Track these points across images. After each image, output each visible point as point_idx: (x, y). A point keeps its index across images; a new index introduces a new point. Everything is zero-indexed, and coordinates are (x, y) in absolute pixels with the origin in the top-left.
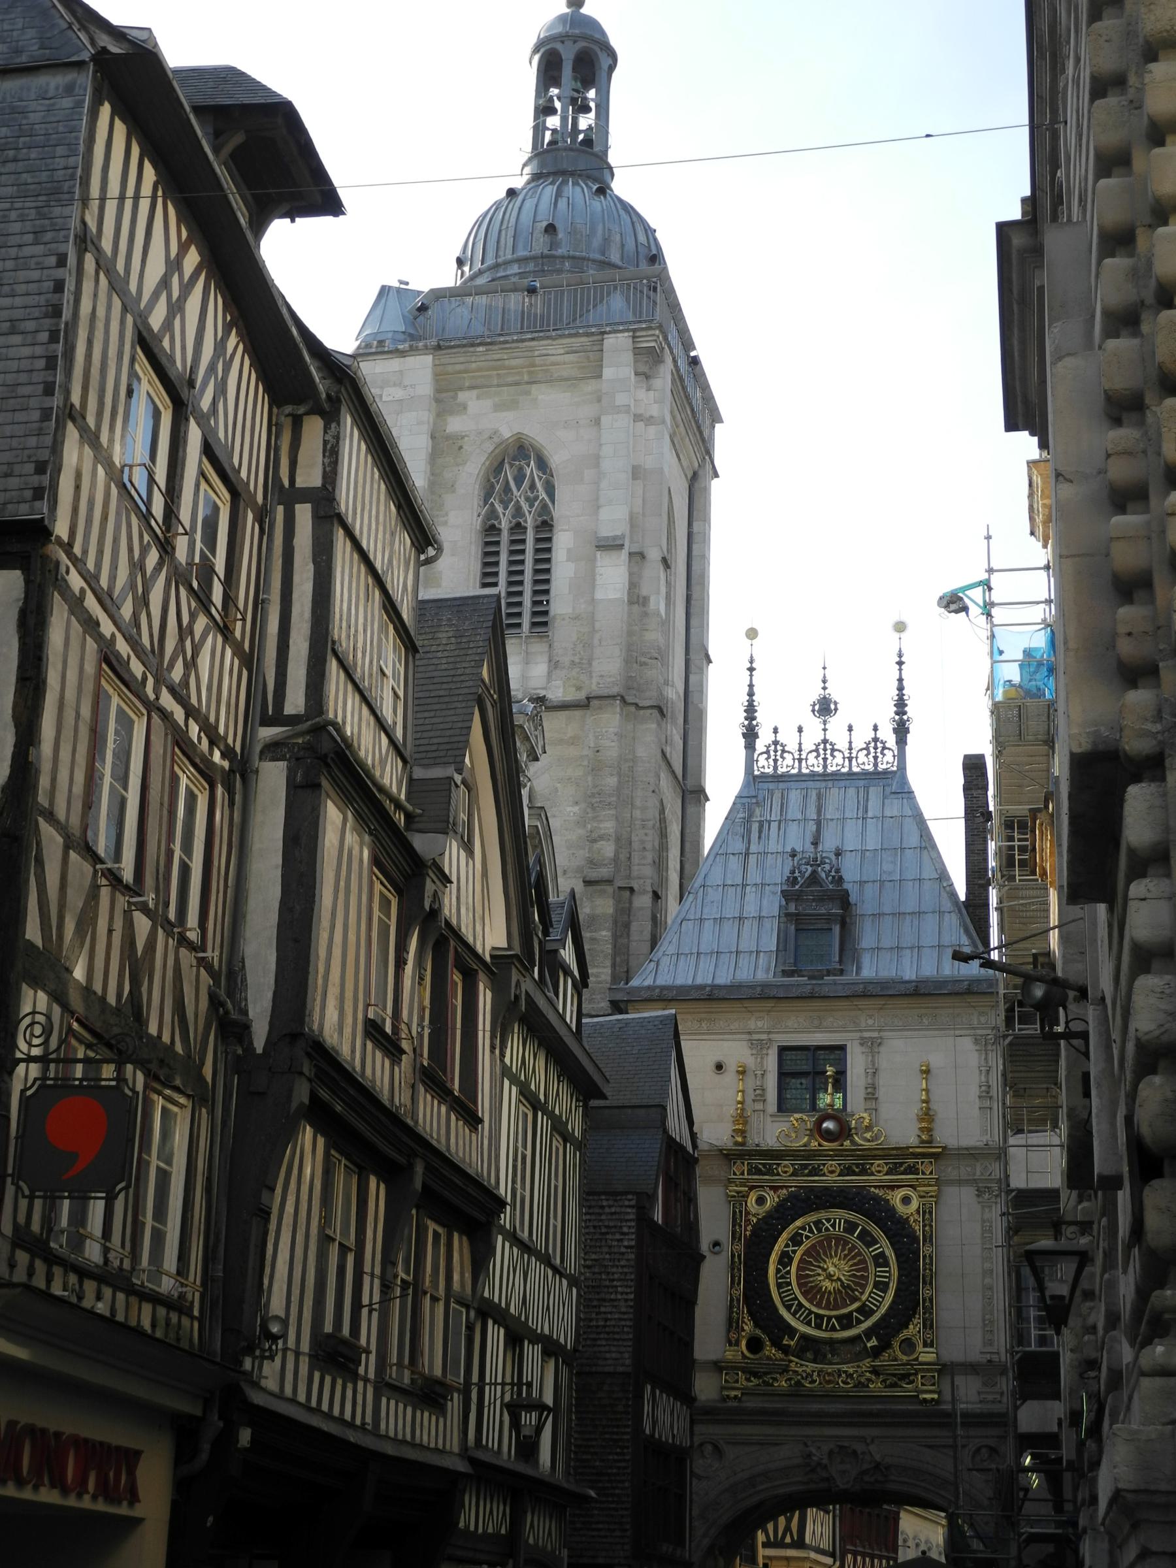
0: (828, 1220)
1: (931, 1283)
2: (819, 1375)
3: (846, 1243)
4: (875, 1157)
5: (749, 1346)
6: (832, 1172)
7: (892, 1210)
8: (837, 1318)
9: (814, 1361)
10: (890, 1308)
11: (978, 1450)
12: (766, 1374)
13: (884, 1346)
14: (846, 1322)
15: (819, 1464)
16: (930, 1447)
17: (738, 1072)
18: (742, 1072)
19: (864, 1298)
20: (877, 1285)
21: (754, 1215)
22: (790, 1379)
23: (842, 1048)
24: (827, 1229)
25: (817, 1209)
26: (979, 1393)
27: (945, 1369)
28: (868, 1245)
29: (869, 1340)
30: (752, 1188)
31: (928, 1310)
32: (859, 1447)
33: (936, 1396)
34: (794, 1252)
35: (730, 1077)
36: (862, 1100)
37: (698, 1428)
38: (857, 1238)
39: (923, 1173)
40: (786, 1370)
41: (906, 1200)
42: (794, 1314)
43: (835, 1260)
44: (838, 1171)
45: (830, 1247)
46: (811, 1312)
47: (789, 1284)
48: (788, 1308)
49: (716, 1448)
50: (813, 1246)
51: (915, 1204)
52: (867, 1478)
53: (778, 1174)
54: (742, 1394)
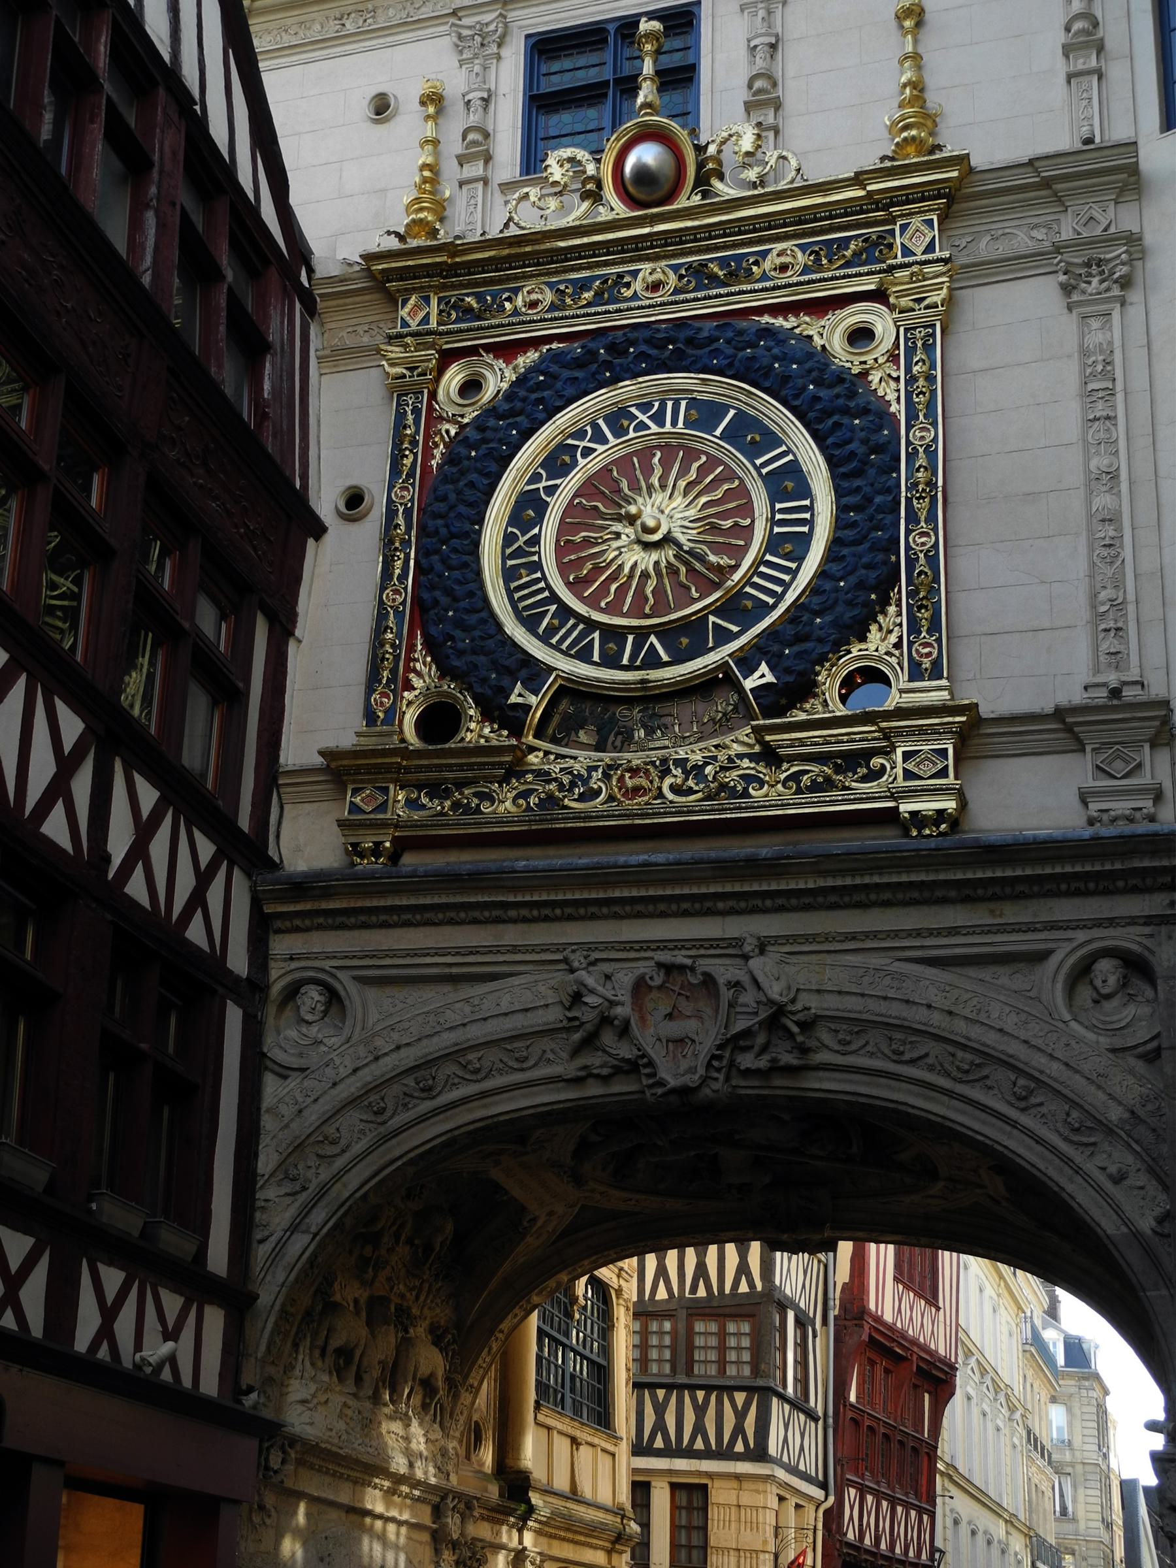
0: (645, 407)
1: (932, 518)
2: (607, 777)
3: (691, 454)
5: (421, 724)
7: (817, 362)
8: (662, 632)
9: (600, 747)
10: (813, 589)
12: (460, 785)
13: (795, 689)
14: (688, 637)
19: (737, 576)
20: (773, 544)
21: (452, 420)
22: (525, 795)
24: (642, 426)
25: (614, 381)
26: (1084, 798)
28: (753, 450)
29: (749, 671)
30: (447, 358)
31: (925, 598)
32: (724, 971)
33: (950, 805)
34: (551, 490)
36: (741, 108)
42: (545, 639)
43: (659, 497)
45: (648, 471)
46: (591, 625)
47: (538, 566)
48: (530, 623)
50: (606, 470)
52: (747, 1061)
53: (516, 312)
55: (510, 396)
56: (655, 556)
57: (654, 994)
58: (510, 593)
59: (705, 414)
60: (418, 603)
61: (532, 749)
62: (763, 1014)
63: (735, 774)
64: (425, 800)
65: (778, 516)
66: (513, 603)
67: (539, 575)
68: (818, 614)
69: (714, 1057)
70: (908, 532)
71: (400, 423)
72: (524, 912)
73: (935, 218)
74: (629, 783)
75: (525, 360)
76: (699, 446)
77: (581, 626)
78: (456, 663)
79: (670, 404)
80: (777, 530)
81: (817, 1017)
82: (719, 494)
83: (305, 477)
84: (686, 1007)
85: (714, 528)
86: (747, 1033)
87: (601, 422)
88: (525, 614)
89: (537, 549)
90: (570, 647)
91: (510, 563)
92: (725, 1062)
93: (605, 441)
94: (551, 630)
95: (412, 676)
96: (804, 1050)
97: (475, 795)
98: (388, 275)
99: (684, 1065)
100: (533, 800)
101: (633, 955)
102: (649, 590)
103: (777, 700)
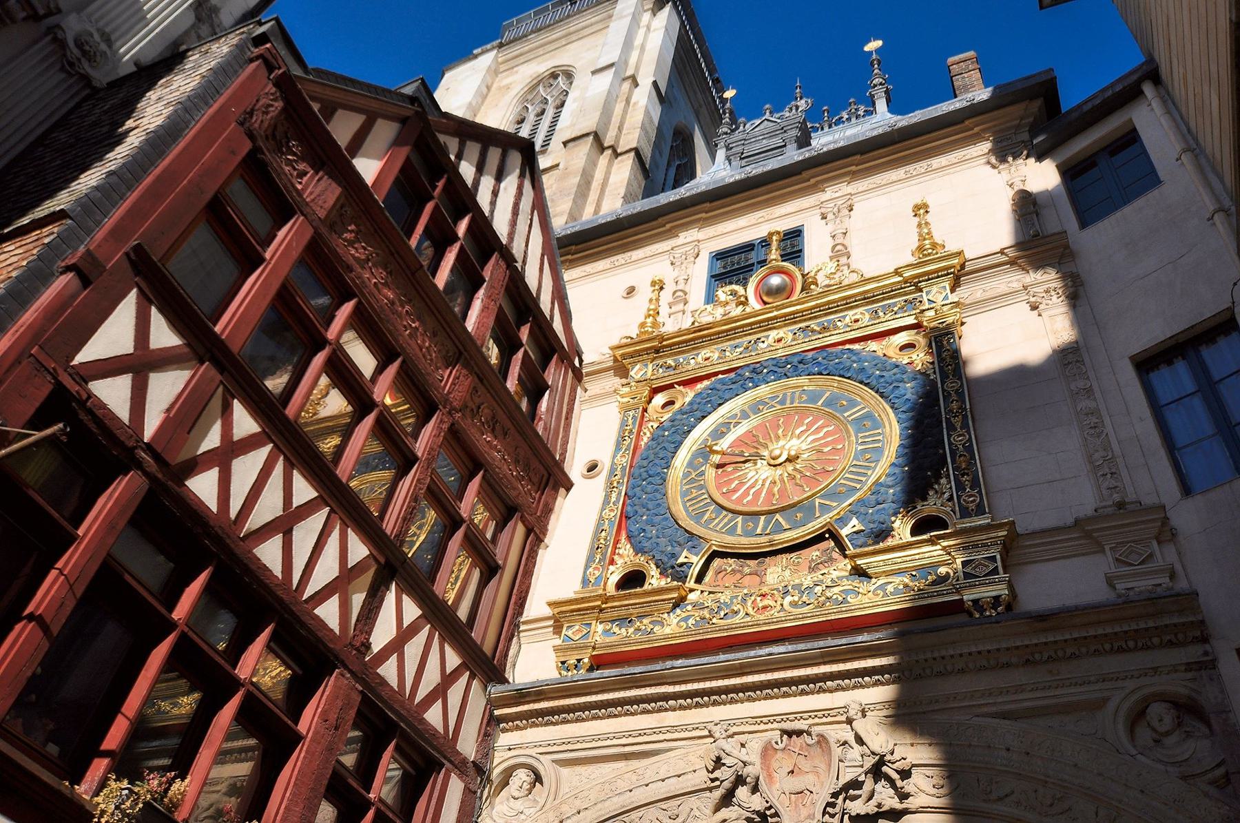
1: (965, 426)
4: (848, 304)
7: (883, 363)
11: (1138, 716)
12: (641, 617)
15: (740, 780)
16: (1004, 716)
17: (653, 283)
18: (659, 286)
22: (686, 619)
23: (795, 235)
30: (656, 391)
33: (1002, 590)
35: (645, 293)
37: (505, 739)
40: (679, 603)
44: (790, 336)
48: (698, 517)
49: (538, 778)
54: (592, 657)
55: (691, 403)
56: (779, 471)
57: (779, 754)
59: (814, 397)
60: (625, 516)
61: (692, 590)
62: (870, 762)
63: (836, 590)
64: (616, 629)
68: (890, 487)
69: (829, 804)
70: (949, 436)
71: (624, 424)
72: (681, 701)
75: (700, 386)
78: (647, 544)
80: (860, 448)
81: (914, 766)
82: (821, 434)
83: (563, 454)
84: (804, 764)
85: (819, 451)
86: (856, 784)
92: (837, 809)
95: (616, 557)
96: (903, 796)
98: (624, 356)
99: (804, 812)
100: (691, 621)
101: (762, 727)
102: (776, 489)
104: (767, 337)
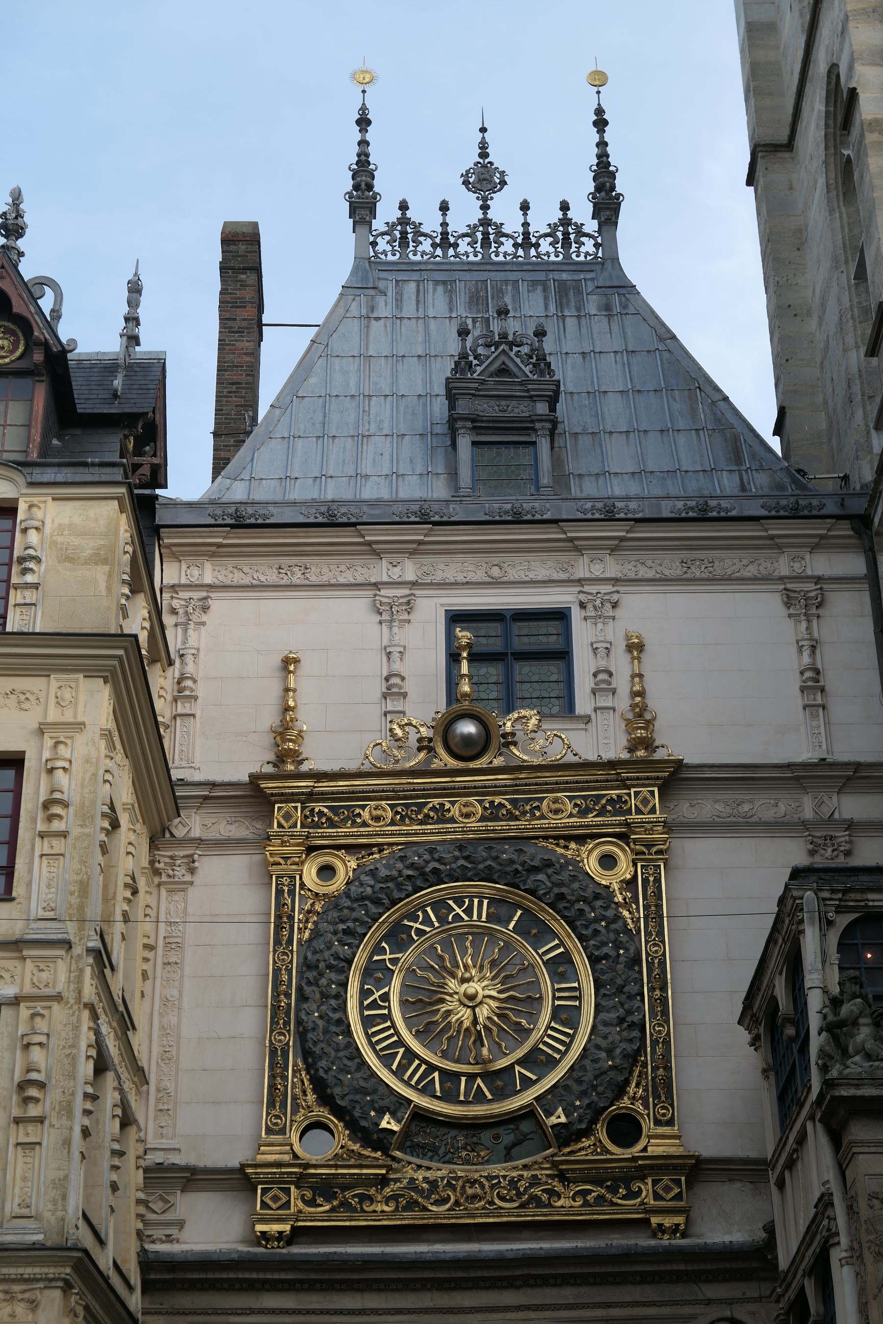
0: (459, 902)
6: (467, 816)
24: (457, 917)
27: (695, 1170)
29: (549, 1114)
38: (515, 930)
39: (639, 811)
41: (607, 861)
42: (398, 1074)
46: (432, 1068)
47: (388, 1017)
48: (386, 1060)
51: (624, 869)
58: (369, 1037)
65: (557, 995)
66: (373, 1045)
67: (389, 1024)
73: (656, 790)
74: (470, 1191)
76: (499, 935)
77: (424, 1067)
79: (476, 901)
80: (557, 1003)
87: (429, 909)
88: (381, 1054)
89: (387, 1004)
90: (418, 1083)
91: (366, 1013)
93: (431, 924)
94: (402, 1068)
97: (354, 1196)
103: (567, 1135)
104: (453, 803)
